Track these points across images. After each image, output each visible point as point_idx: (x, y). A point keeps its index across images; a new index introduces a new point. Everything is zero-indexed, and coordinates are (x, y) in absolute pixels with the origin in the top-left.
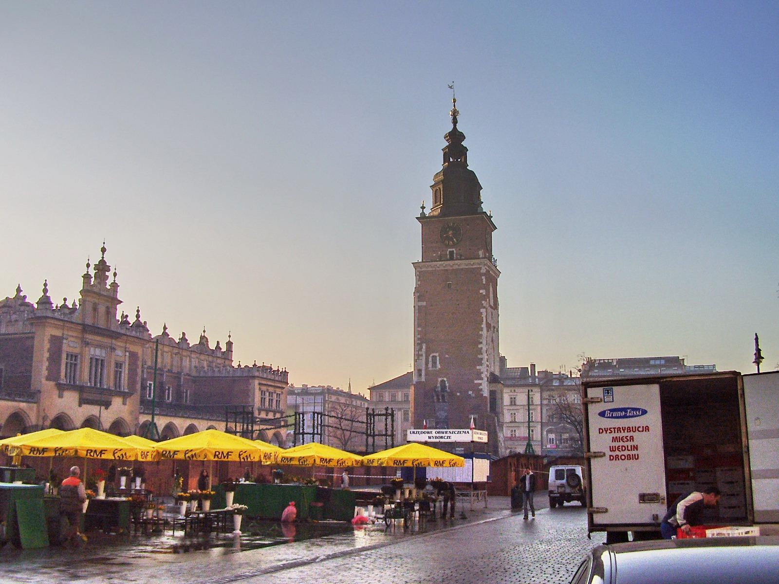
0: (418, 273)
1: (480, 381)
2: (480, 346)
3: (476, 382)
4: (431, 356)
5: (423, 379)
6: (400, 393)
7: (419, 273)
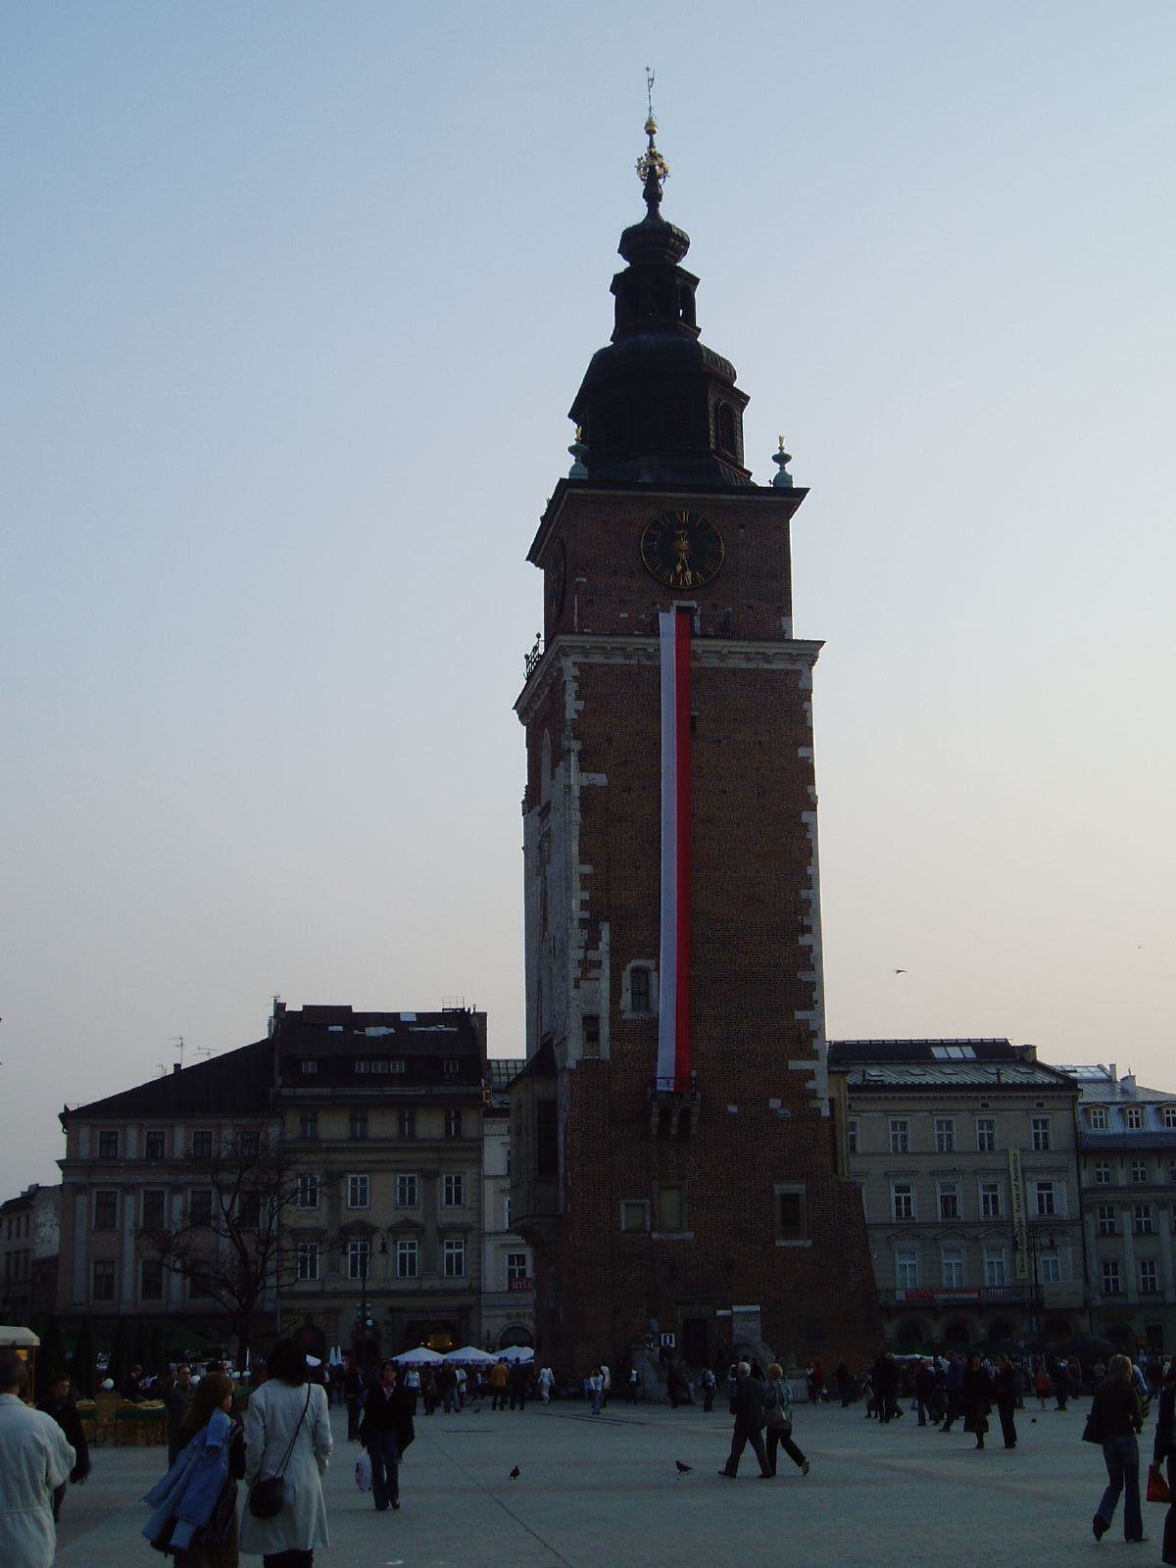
0: (577, 673)
1: (806, 1065)
2: (804, 940)
3: (794, 1065)
4: (629, 967)
5: (605, 1050)
6: (132, 1134)
7: (581, 670)
